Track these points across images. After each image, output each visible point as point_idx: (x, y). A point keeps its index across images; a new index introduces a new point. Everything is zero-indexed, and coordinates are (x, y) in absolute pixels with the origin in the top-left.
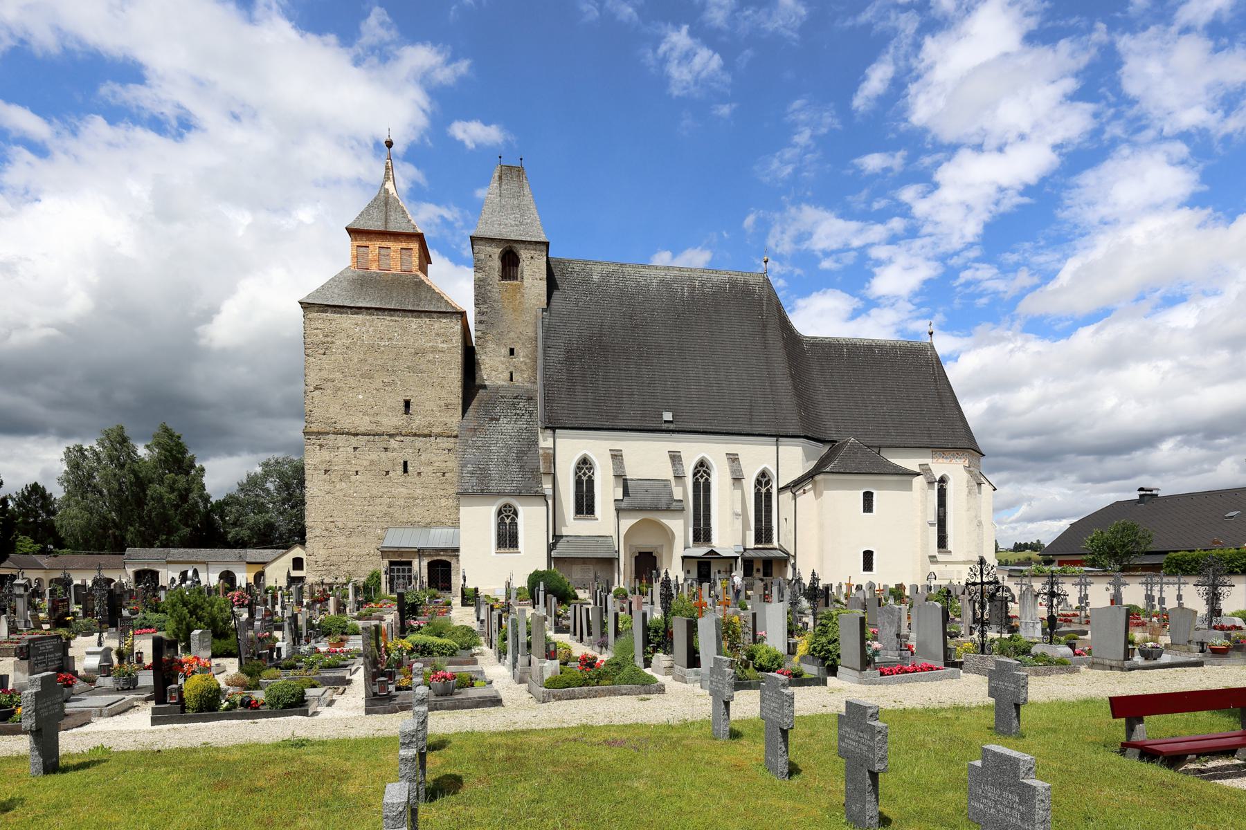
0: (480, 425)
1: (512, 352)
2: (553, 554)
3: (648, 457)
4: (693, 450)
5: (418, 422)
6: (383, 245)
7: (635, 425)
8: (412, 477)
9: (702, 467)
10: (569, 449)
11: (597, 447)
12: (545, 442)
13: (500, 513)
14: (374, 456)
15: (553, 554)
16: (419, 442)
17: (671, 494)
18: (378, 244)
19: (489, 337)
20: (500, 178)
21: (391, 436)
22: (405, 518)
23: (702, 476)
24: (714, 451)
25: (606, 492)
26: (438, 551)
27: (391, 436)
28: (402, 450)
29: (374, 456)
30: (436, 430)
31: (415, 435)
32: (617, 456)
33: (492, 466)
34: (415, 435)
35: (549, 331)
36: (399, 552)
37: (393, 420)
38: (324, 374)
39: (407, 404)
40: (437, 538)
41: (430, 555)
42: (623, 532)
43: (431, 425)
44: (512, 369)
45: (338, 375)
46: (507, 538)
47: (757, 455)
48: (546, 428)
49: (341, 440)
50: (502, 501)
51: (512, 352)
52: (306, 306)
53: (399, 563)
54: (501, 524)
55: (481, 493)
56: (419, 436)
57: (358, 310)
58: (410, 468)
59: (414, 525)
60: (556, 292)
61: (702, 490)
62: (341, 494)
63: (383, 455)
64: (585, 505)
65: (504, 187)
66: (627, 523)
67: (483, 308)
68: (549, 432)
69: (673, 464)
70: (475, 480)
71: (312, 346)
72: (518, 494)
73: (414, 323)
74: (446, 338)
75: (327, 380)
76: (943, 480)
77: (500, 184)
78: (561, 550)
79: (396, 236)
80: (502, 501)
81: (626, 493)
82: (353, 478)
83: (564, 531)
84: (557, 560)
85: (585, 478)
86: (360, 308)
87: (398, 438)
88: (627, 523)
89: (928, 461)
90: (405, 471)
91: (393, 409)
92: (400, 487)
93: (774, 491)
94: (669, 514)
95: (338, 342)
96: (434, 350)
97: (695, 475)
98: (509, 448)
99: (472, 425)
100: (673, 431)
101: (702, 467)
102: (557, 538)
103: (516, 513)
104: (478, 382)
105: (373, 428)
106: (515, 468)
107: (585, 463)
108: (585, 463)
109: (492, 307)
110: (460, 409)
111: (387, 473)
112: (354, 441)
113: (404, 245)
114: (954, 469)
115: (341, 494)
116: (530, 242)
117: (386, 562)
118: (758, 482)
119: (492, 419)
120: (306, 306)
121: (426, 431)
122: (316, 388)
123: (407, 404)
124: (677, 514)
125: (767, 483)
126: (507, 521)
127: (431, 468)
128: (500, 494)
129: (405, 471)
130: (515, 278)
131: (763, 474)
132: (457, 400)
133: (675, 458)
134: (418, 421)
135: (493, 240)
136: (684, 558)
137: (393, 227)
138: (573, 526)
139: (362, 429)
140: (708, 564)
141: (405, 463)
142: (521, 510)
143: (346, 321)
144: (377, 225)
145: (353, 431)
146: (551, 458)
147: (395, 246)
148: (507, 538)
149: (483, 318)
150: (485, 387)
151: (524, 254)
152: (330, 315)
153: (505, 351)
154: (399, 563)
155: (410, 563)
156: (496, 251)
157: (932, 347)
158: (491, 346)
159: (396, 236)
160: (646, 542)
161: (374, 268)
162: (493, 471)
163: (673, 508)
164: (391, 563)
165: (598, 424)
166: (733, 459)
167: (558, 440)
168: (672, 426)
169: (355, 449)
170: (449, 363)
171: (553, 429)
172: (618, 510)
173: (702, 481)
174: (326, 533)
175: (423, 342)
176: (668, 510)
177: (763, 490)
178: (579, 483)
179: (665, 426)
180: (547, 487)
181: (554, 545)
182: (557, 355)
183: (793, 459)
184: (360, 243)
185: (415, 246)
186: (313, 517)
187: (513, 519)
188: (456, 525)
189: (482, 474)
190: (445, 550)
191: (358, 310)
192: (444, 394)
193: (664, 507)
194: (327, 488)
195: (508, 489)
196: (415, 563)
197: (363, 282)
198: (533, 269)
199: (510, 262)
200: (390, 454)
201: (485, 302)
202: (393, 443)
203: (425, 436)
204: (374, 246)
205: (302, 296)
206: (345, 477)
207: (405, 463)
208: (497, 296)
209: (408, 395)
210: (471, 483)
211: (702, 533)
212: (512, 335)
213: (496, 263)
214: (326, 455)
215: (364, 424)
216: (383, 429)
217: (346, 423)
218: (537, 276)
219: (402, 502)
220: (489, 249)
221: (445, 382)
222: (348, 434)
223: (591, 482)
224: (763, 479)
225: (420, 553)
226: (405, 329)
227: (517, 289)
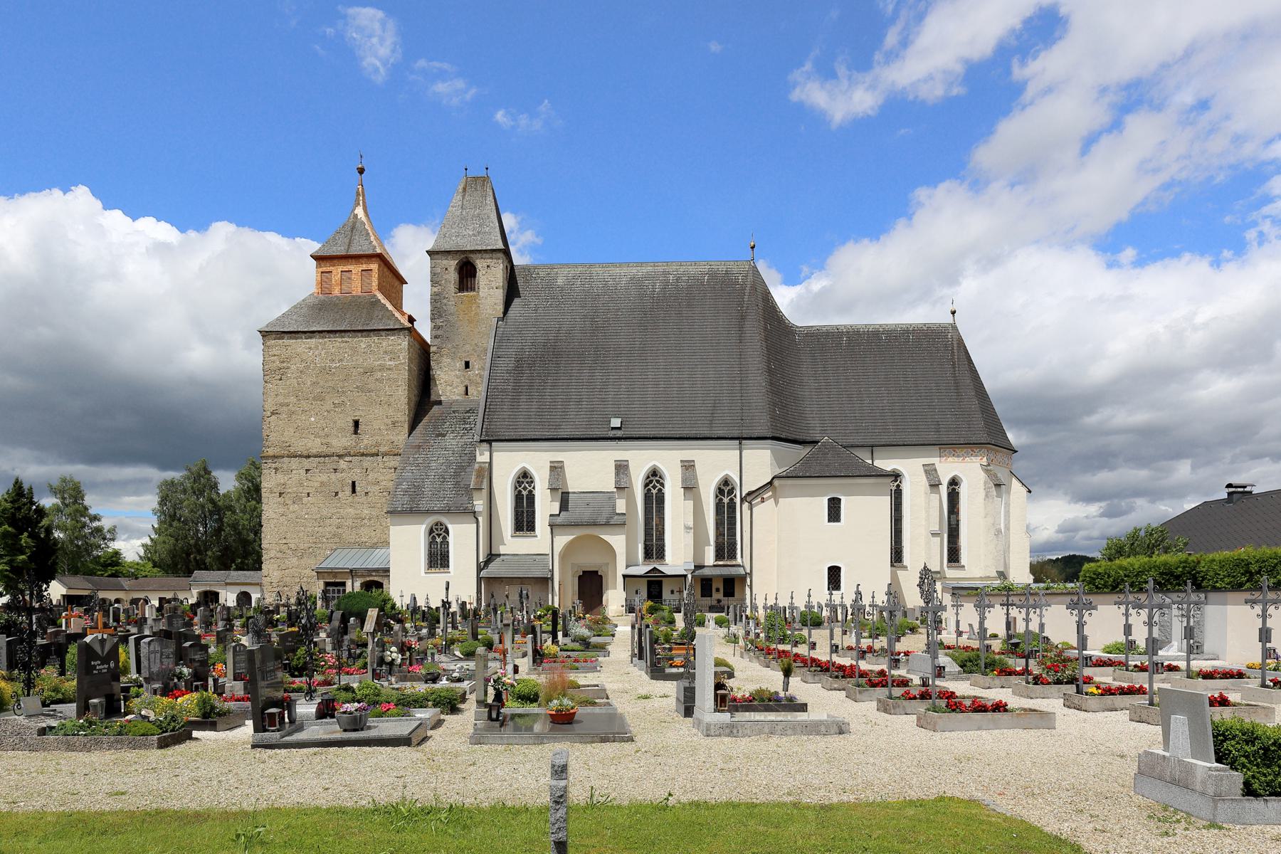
0: (426, 441)
1: (467, 365)
2: (483, 574)
3: (590, 469)
4: (641, 459)
5: (366, 442)
6: (345, 269)
7: (578, 434)
8: (359, 496)
9: (654, 477)
10: (507, 463)
11: (537, 460)
12: (482, 457)
13: (431, 531)
14: (324, 478)
15: (483, 574)
16: (367, 462)
17: (614, 507)
18: (340, 269)
19: (445, 351)
20: (464, 189)
21: (340, 456)
22: (352, 538)
23: (654, 487)
24: (668, 459)
25: (545, 506)
26: (370, 571)
27: (340, 456)
28: (350, 470)
29: (324, 478)
30: (382, 449)
31: (363, 455)
32: (557, 469)
33: (427, 483)
34: (363, 455)
35: (500, 340)
36: (333, 572)
37: (343, 441)
38: (281, 399)
39: (356, 424)
40: (373, 560)
41: (362, 576)
42: (558, 550)
43: (378, 445)
44: (467, 382)
45: (293, 399)
46: (438, 558)
47: (715, 463)
48: (482, 441)
49: (294, 463)
50: (431, 520)
51: (467, 365)
52: (265, 334)
53: (334, 585)
54: (432, 543)
55: (407, 511)
56: (366, 455)
57: (312, 333)
58: (358, 489)
59: (361, 545)
60: (516, 301)
61: (654, 501)
62: (294, 516)
63: (333, 476)
64: (524, 522)
65: (467, 198)
66: (562, 540)
67: (439, 322)
68: (485, 445)
69: (617, 474)
70: (406, 498)
71: (272, 372)
72: (447, 511)
73: (363, 343)
74: (393, 355)
75: (282, 405)
76: (954, 482)
77: (463, 197)
78: (494, 570)
79: (357, 258)
80: (431, 520)
81: (564, 506)
82: (305, 500)
83: (503, 550)
84: (489, 580)
85: (525, 493)
86: (313, 332)
87: (347, 459)
88: (562, 540)
90: (354, 491)
91: (342, 430)
92: (349, 508)
93: (738, 500)
94: (608, 529)
95: (293, 367)
96: (382, 368)
98: (449, 464)
99: (417, 442)
100: (619, 439)
101: (654, 477)
102: (491, 557)
103: (447, 531)
104: (433, 398)
105: (324, 449)
106: (450, 485)
107: (524, 477)
108: (524, 477)
109: (448, 321)
110: (406, 426)
111: (337, 494)
112: (307, 463)
113: (364, 267)
114: (969, 470)
115: (294, 516)
116: (486, 251)
117: (321, 584)
119: (438, 435)
120: (265, 334)
121: (374, 451)
122: (273, 413)
123: (356, 424)
124: (617, 529)
125: (731, 491)
126: (438, 540)
127: (377, 488)
128: (429, 512)
129: (354, 491)
130: (473, 289)
131: (726, 482)
132: (403, 417)
133: (622, 468)
134: (366, 441)
135: (449, 252)
136: (625, 576)
137: (355, 250)
138: (512, 544)
139: (314, 451)
140: (660, 584)
141: (354, 483)
142: (450, 527)
143: (300, 345)
144: (339, 250)
145: (305, 453)
146: (487, 472)
147: (356, 269)
148: (438, 558)
149: (439, 332)
150: (440, 403)
151: (480, 264)
152: (286, 342)
153: (461, 365)
154: (334, 585)
155: (343, 584)
156: (452, 264)
158: (446, 360)
159: (357, 258)
160: (590, 561)
161: (336, 292)
162: (427, 491)
163: (616, 522)
164: (327, 584)
165: (537, 434)
166: (688, 466)
167: (495, 454)
168: (619, 434)
169: (307, 471)
170: (396, 380)
171: (489, 442)
172: (551, 526)
173: (654, 492)
174: (279, 555)
175: (372, 361)
176: (607, 524)
177: (726, 500)
178: (518, 498)
179: (611, 434)
180: (479, 504)
181: (487, 563)
182: (506, 364)
183: (759, 464)
184: (324, 269)
185: (374, 266)
186: (269, 539)
187: (445, 538)
188: (386, 544)
189: (416, 491)
190: (377, 570)
191: (312, 333)
192: (391, 412)
193: (603, 521)
194: (281, 510)
195: (438, 505)
196: (349, 583)
197: (323, 305)
198: (491, 278)
199: (467, 273)
200: (339, 475)
201: (441, 316)
202: (343, 464)
203: (373, 455)
204: (337, 270)
205: (262, 326)
206: (297, 500)
207: (354, 483)
208: (452, 309)
209: (357, 415)
210: (403, 501)
211: (654, 549)
212: (468, 347)
213: (453, 276)
214: (281, 478)
215: (315, 445)
216: (333, 450)
217: (299, 446)
218: (494, 284)
219: (349, 522)
220: (445, 262)
221: (392, 400)
222: (300, 456)
223: (531, 498)
224: (725, 488)
225: (353, 573)
226: (354, 350)
227: (475, 298)
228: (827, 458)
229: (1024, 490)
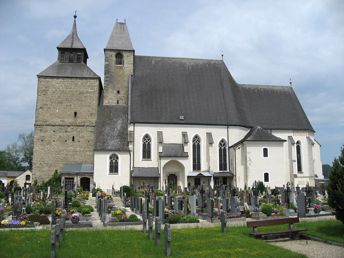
1: (118, 92)
3: (173, 134)
4: (192, 131)
7: (168, 121)
8: (76, 143)
9: (197, 138)
10: (140, 132)
11: (152, 131)
12: (131, 128)
13: (111, 158)
14: (61, 134)
16: (79, 129)
19: (110, 86)
21: (68, 126)
23: (196, 142)
24: (202, 132)
26: (85, 173)
27: (68, 126)
28: (72, 132)
29: (61, 134)
30: (86, 124)
31: (78, 126)
32: (160, 134)
34: (78, 126)
37: (69, 120)
38: (44, 102)
39: (76, 113)
40: (85, 169)
42: (162, 166)
43: (84, 122)
44: (118, 99)
46: (114, 168)
47: (219, 134)
48: (131, 123)
51: (118, 92)
52: (39, 77)
54: (111, 163)
56: (79, 126)
58: (75, 139)
61: (197, 148)
63: (65, 134)
64: (147, 154)
66: (164, 162)
67: (108, 75)
75: (45, 105)
76: (298, 142)
80: (111, 153)
82: (53, 143)
85: (147, 143)
88: (164, 162)
89: (291, 134)
90: (73, 140)
93: (227, 148)
94: (182, 158)
95: (50, 90)
96: (87, 92)
97: (193, 142)
101: (197, 138)
103: (117, 158)
105: (62, 123)
107: (147, 138)
108: (147, 138)
109: (111, 75)
111: (66, 141)
116: (127, 51)
118: (220, 144)
120: (39, 77)
121: (83, 124)
122: (41, 108)
123: (76, 113)
125: (224, 145)
127: (83, 139)
128: (111, 150)
129: (73, 140)
131: (222, 141)
133: (185, 135)
134: (79, 121)
139: (57, 124)
140: (199, 180)
141: (73, 137)
142: (119, 156)
143: (54, 82)
145: (54, 124)
148: (114, 168)
151: (125, 55)
153: (116, 92)
155: (73, 179)
156: (114, 54)
157: (291, 88)
158: (110, 90)
160: (173, 170)
166: (209, 135)
168: (183, 122)
170: (92, 97)
171: (134, 123)
173: (196, 144)
177: (223, 148)
178: (144, 145)
179: (181, 122)
183: (236, 134)
190: (87, 173)
191: (58, 78)
192: (90, 110)
196: (75, 178)
200: (67, 134)
201: (108, 73)
202: (69, 129)
206: (49, 143)
207: (73, 137)
208: (113, 71)
209: (76, 110)
211: (197, 166)
214: (43, 134)
215: (58, 121)
217: (51, 122)
219: (71, 153)
222: (51, 125)
223: (149, 145)
224: (222, 143)
225: (77, 174)
226: (76, 85)
228: (260, 135)
229: (319, 146)
